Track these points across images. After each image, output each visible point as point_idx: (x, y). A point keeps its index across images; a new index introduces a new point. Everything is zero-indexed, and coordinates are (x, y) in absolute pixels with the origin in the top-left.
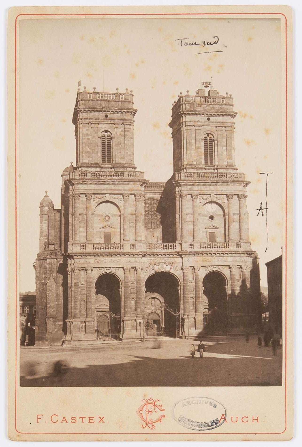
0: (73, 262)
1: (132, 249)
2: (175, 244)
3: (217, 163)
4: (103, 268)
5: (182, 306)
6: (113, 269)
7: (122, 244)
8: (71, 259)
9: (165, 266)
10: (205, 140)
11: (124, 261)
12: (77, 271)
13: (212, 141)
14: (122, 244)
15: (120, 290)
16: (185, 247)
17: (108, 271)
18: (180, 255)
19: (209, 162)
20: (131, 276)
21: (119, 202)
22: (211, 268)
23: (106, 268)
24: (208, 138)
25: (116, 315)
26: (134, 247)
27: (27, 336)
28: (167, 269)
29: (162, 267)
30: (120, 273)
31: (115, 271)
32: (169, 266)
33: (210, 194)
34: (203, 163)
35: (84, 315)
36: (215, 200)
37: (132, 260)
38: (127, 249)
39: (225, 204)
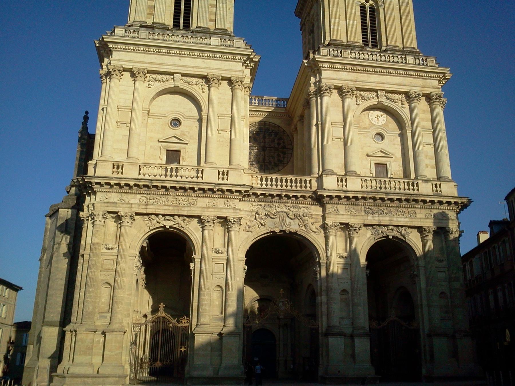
0: (93, 201)
1: (221, 179)
2: (308, 179)
3: (384, 44)
4: (157, 215)
5: (324, 308)
6: (179, 220)
7: (200, 169)
8: (89, 195)
9: (288, 220)
10: (363, 8)
11: (202, 205)
12: (99, 219)
13: (374, 11)
14: (200, 169)
15: (192, 265)
16: (330, 183)
17: (168, 224)
18: (319, 199)
19: (370, 44)
20: (216, 235)
21: (200, 91)
22: (385, 229)
23: (164, 215)
24: (368, 5)
25: (178, 322)
26: (225, 176)
27: (18, 363)
28: (293, 226)
29: (283, 222)
30: (192, 230)
31: (182, 222)
32: (297, 221)
33: (376, 91)
34: (361, 41)
35: (106, 317)
36: (386, 102)
37: (220, 202)
38: (211, 177)
39: (405, 112)
